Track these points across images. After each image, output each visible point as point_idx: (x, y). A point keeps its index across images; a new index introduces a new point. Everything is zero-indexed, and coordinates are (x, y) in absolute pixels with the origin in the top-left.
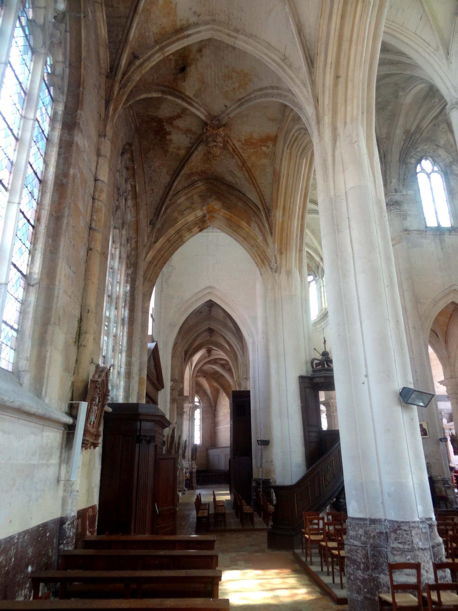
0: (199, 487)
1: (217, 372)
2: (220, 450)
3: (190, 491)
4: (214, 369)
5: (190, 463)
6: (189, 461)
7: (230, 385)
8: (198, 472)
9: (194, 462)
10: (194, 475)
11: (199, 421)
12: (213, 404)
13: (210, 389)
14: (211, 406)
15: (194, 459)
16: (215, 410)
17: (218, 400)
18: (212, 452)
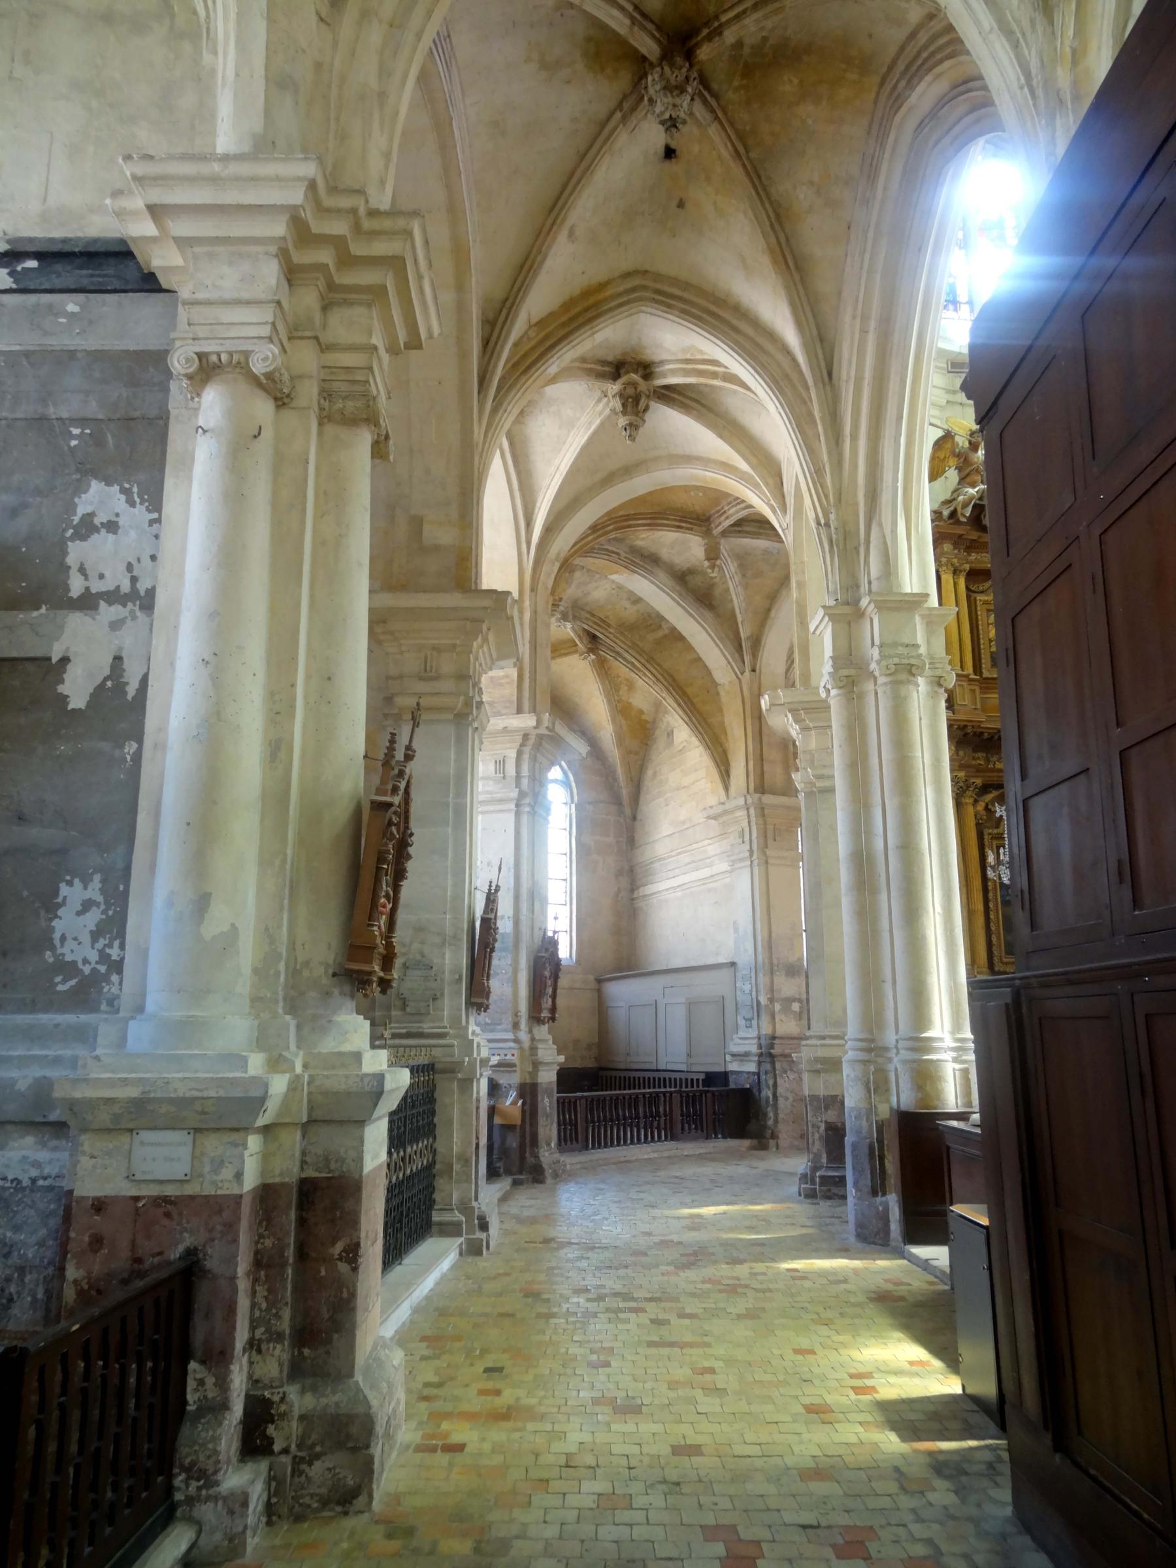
0: (571, 1160)
1: (653, 621)
2: (661, 981)
3: (527, 1201)
4: (637, 600)
5: (523, 1035)
6: (516, 1026)
7: (715, 684)
8: (568, 1079)
9: (542, 1031)
10: (547, 1104)
11: (564, 861)
12: (625, 793)
13: (614, 720)
14: (617, 801)
15: (545, 1014)
16: (634, 818)
17: (650, 772)
18: (622, 992)
